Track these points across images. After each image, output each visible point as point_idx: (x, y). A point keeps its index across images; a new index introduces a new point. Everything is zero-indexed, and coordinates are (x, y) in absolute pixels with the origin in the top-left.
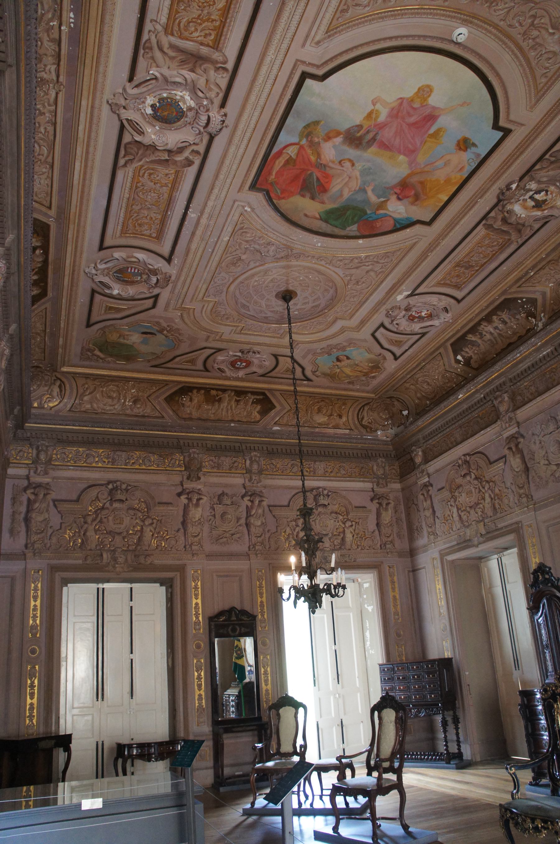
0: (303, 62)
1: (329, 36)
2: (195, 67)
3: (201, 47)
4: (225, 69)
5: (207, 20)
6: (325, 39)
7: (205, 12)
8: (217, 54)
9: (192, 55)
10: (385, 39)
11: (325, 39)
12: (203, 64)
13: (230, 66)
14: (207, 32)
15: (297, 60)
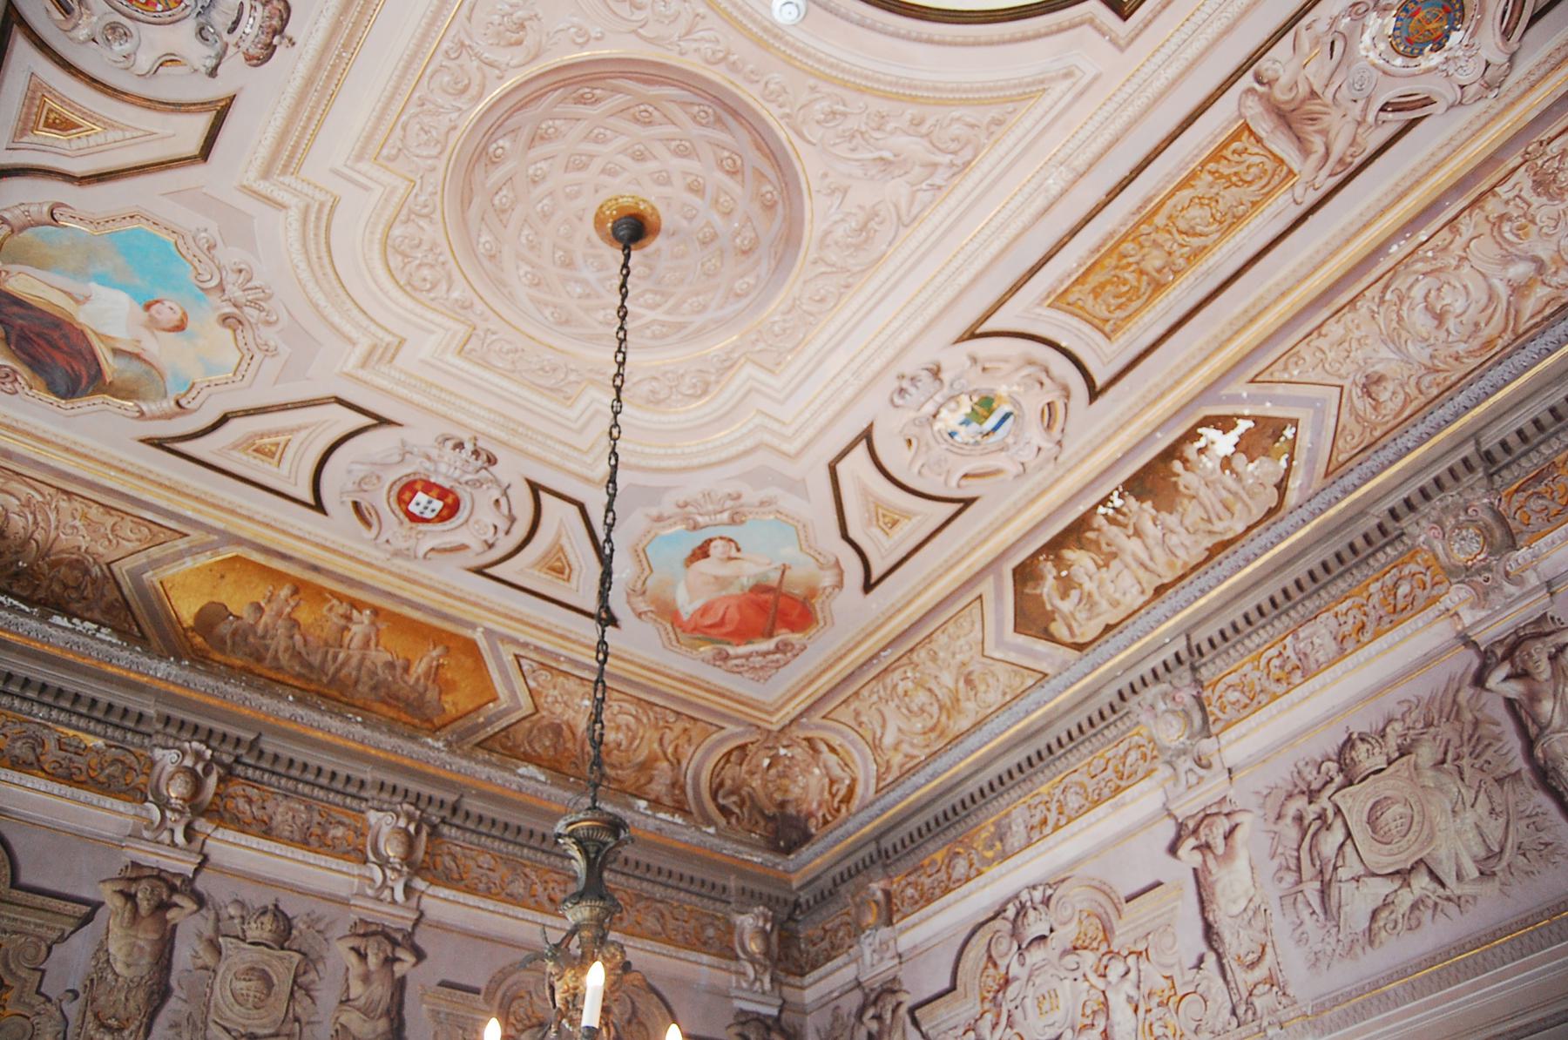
0: (1113, 41)
1: (1042, 82)
2: (1303, 101)
3: (1263, 134)
4: (1258, 79)
5: (1222, 176)
6: (1052, 79)
7: (1214, 190)
8: (1248, 113)
9: (1290, 127)
10: (942, 43)
11: (1052, 79)
12: (1287, 102)
13: (1247, 80)
14: (1236, 158)
15: (1122, 49)
